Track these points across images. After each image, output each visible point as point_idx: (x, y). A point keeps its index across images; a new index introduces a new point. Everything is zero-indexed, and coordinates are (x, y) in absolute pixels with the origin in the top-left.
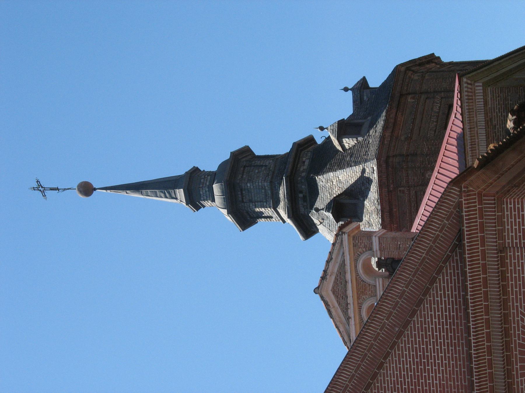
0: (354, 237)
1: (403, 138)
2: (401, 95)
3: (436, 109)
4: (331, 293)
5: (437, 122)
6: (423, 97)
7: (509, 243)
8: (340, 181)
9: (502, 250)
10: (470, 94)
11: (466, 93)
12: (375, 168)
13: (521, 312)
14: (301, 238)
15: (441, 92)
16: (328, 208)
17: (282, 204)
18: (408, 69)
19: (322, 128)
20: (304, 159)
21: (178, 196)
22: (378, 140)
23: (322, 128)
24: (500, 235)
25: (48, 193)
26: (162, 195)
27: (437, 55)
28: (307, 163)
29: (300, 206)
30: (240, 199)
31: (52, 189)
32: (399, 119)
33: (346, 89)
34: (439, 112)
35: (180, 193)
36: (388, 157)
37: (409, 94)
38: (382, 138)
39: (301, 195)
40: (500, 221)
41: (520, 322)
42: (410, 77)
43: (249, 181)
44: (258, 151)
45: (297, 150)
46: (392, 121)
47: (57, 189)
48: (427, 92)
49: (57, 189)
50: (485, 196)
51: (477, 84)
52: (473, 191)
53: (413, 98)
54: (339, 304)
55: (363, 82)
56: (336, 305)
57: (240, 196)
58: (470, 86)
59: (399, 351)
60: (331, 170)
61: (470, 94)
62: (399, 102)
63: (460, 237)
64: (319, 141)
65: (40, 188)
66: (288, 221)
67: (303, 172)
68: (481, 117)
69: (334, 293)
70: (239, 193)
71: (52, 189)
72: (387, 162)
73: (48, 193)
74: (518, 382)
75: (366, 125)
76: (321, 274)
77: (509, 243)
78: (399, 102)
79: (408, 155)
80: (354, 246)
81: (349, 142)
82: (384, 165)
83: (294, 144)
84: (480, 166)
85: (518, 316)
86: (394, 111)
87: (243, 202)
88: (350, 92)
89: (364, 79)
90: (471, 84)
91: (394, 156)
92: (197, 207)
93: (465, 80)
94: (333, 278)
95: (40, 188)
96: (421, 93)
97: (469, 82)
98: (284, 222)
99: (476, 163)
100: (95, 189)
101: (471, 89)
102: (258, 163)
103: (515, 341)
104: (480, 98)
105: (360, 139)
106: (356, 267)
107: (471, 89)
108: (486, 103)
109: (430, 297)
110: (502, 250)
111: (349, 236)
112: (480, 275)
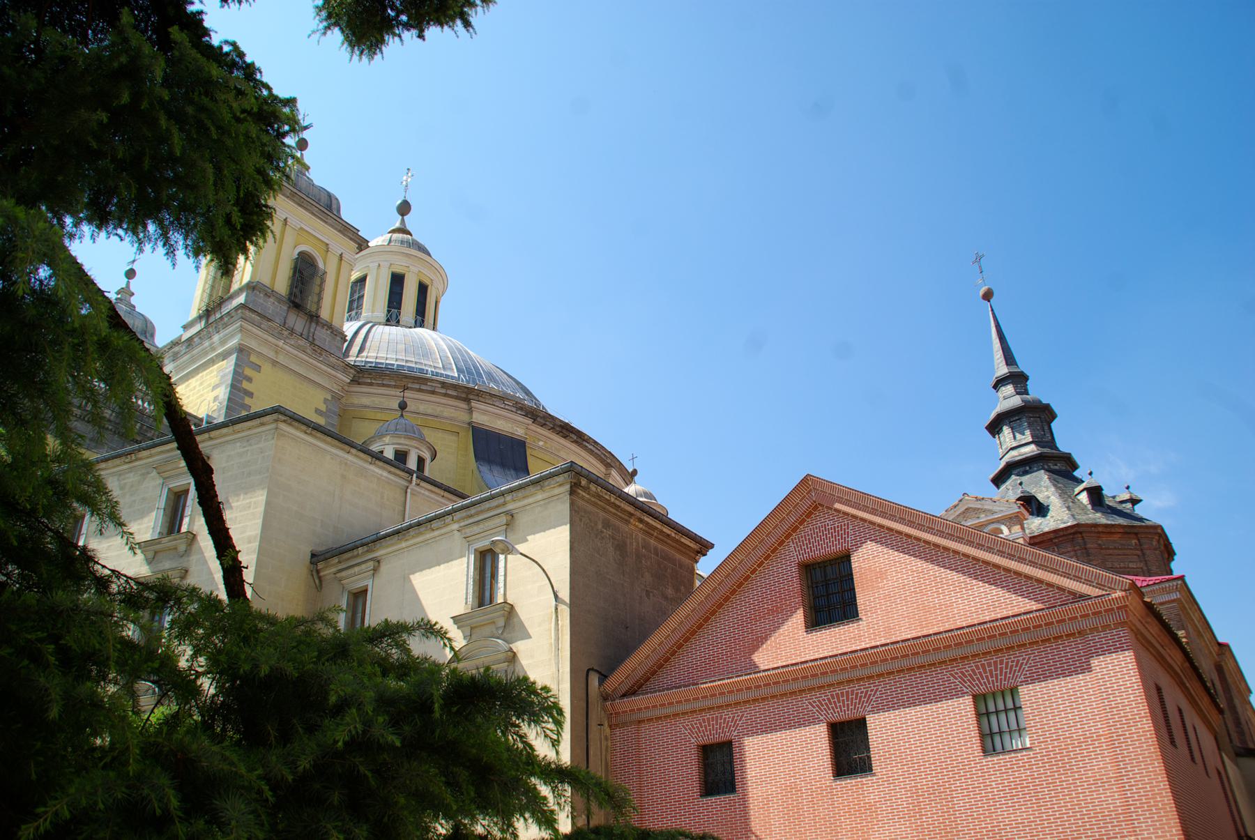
0: (1017, 516)
1: (1100, 542)
2: (1136, 534)
3: (1131, 565)
4: (966, 507)
5: (1121, 568)
6: (1139, 552)
7: (1088, 637)
8: (1049, 497)
9: (1081, 633)
10: (1168, 589)
11: (1167, 586)
12: (1069, 524)
13: (1029, 658)
14: (992, 476)
15: (1147, 566)
18: (1160, 535)
19: (1091, 474)
20: (1059, 465)
22: (1093, 522)
24: (1095, 629)
25: (976, 265)
27: (1175, 557)
29: (1018, 470)
30: (1012, 420)
32: (1115, 536)
34: (1128, 568)
36: (1081, 533)
37: (1138, 540)
38: (1096, 525)
39: (1028, 468)
41: (1021, 658)
42: (1153, 538)
44: (1054, 425)
45: (1066, 457)
46: (1113, 531)
48: (1144, 554)
50: (1126, 611)
51: (1178, 593)
52: (1128, 599)
53: (1136, 545)
54: (958, 516)
56: (957, 513)
57: (1014, 419)
58: (1175, 587)
59: (972, 565)
61: (1168, 589)
62: (1130, 533)
64: (1076, 473)
65: (979, 259)
66: (1002, 464)
67: (1048, 466)
69: (966, 509)
70: (1017, 418)
73: (976, 265)
74: (970, 664)
77: (1088, 637)
78: (1130, 533)
79: (1086, 549)
80: (1010, 518)
81: (1084, 497)
82: (1072, 531)
83: (1070, 454)
84: (1146, 603)
85: (1026, 655)
86: (1121, 530)
90: (1177, 588)
91: (1083, 537)
93: (1180, 582)
94: (979, 506)
95: (979, 259)
96: (1142, 550)
97: (1179, 586)
98: (1001, 459)
99: (1147, 599)
100: (989, 301)
101: (1173, 589)
102: (1046, 428)
103: (1005, 656)
105: (1089, 507)
106: (993, 523)
107: (1173, 589)
109: (1024, 582)
110: (1081, 633)
111: (1018, 512)
112: (1055, 618)
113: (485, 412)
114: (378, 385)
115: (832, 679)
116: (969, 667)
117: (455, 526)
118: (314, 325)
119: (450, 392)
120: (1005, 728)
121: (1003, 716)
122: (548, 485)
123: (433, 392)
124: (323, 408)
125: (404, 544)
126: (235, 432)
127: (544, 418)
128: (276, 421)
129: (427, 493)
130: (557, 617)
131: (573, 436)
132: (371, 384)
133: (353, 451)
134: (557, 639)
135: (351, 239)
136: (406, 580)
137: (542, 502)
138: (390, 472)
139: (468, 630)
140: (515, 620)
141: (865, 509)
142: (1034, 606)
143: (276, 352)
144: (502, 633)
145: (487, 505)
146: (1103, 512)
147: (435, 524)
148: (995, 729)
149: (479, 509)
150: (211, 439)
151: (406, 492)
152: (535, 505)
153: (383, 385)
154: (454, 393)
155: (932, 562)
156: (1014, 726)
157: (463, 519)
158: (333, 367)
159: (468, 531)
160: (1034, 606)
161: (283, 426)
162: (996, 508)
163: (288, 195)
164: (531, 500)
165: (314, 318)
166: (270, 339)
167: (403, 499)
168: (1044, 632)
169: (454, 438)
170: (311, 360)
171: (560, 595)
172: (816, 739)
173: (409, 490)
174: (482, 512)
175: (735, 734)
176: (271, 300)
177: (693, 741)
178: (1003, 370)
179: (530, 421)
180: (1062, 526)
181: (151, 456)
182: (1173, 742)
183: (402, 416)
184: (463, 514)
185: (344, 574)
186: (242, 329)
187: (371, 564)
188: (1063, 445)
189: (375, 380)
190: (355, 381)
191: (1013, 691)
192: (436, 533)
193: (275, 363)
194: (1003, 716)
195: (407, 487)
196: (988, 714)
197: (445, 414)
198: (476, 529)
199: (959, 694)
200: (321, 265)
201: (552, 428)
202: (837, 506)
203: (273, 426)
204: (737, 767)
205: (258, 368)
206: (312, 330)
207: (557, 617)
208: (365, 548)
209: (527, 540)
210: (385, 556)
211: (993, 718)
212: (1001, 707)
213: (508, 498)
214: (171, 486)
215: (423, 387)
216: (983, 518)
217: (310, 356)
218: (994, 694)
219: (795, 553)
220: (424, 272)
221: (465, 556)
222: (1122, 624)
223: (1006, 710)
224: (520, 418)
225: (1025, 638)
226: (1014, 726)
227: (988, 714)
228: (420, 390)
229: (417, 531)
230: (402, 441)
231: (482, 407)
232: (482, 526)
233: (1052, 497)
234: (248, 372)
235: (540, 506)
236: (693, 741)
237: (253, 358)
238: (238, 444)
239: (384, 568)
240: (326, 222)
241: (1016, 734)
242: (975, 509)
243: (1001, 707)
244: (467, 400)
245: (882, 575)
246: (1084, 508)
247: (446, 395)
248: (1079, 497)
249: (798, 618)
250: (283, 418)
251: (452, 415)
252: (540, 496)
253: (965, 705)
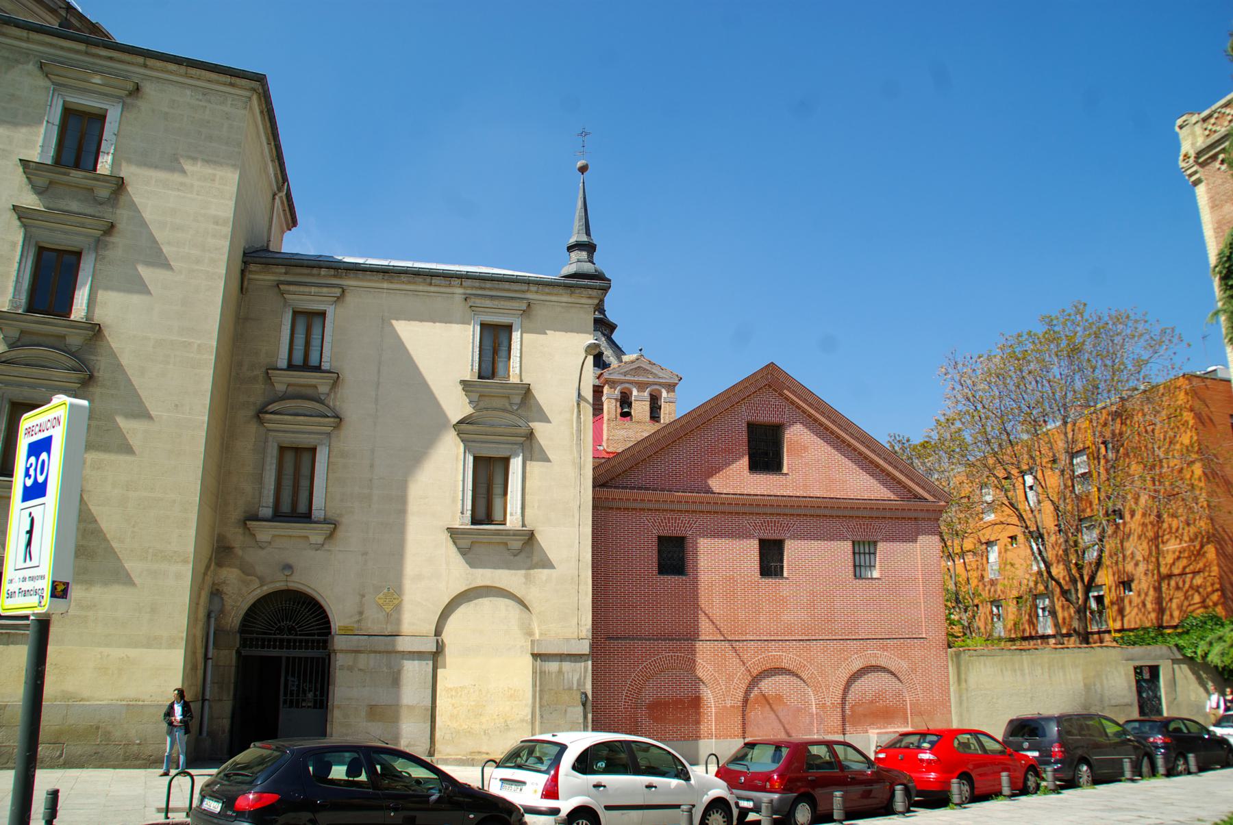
35: (584, 238)
40: (929, 519)
54: (632, 369)
73: (581, 139)
76: (653, 361)
94: (649, 368)
115: (769, 510)
116: (853, 523)
117: (460, 291)
120: (863, 564)
121: (862, 556)
122: (580, 293)
125: (385, 285)
126: (186, 75)
128: (254, 90)
130: (579, 411)
134: (579, 431)
136: (384, 323)
137: (564, 304)
139: (475, 397)
140: (532, 401)
141: (805, 401)
142: (893, 497)
144: (517, 410)
145: (507, 286)
147: (435, 280)
149: (497, 286)
150: (145, 66)
152: (556, 304)
155: (838, 450)
156: (868, 564)
157: (472, 288)
159: (478, 302)
160: (893, 497)
162: (661, 375)
164: (554, 298)
168: (899, 514)
171: (583, 393)
172: (750, 549)
174: (497, 289)
175: (690, 533)
177: (654, 532)
178: (577, 237)
181: (28, 40)
184: (477, 283)
185: (292, 288)
187: (338, 292)
191: (875, 543)
192: (432, 289)
194: (862, 556)
198: (488, 303)
199: (844, 539)
202: (785, 391)
203: (248, 94)
204: (690, 556)
207: (579, 411)
208: (332, 272)
209: (546, 334)
210: (351, 288)
213: (533, 288)
214: (68, 99)
216: (651, 379)
218: (864, 542)
219: (746, 414)
221: (470, 324)
225: (888, 514)
226: (868, 564)
229: (411, 279)
232: (496, 303)
235: (562, 307)
236: (654, 532)
238: (188, 92)
239: (350, 299)
241: (868, 569)
242: (645, 369)
245: (805, 448)
249: (745, 461)
252: (565, 299)
253: (848, 545)
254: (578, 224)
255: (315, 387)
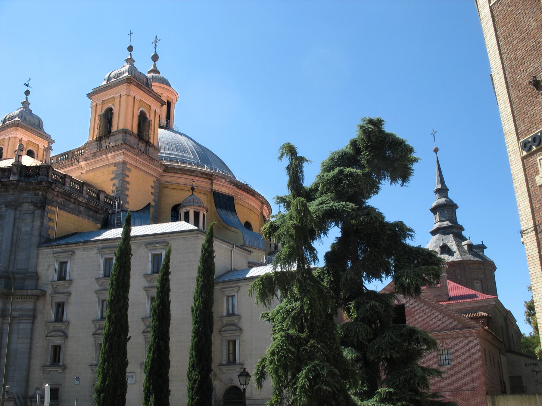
8: (452, 246)
9: (467, 337)
12: (459, 259)
16: (443, 244)
17: (441, 223)
19: (469, 238)
21: (438, 185)
23: (469, 238)
26: (438, 179)
28: (456, 231)
31: (434, 137)
33: (482, 242)
35: (440, 186)
36: (463, 263)
38: (469, 261)
39: (445, 230)
43: (447, 211)
47: (434, 139)
48: (485, 272)
49: (434, 139)
55: (486, 248)
60: (456, 242)
63: (470, 328)
68: (485, 304)
71: (434, 137)
72: (462, 263)
75: (472, 253)
81: (466, 247)
83: (462, 226)
87: (440, 210)
88: (482, 243)
89: (486, 248)
92: (435, 192)
95: (434, 133)
98: (434, 224)
102: (454, 213)
104: (490, 303)
105: (467, 252)
108: (489, 305)
110: (467, 337)
113: (218, 185)
114: (174, 173)
118: (148, 147)
119: (204, 176)
123: (197, 176)
124: (153, 185)
126: (179, 235)
127: (241, 186)
128: (197, 234)
129: (237, 251)
131: (251, 192)
132: (171, 172)
133: (218, 240)
135: (159, 102)
138: (228, 246)
143: (136, 162)
146: (472, 255)
148: (442, 359)
150: (169, 236)
151: (232, 252)
153: (176, 173)
154: (206, 177)
158: (157, 166)
161: (200, 235)
163: (135, 84)
165: (148, 143)
166: (134, 156)
167: (231, 254)
169: (205, 196)
170: (149, 164)
173: (232, 251)
176: (132, 137)
179: (235, 188)
180: (457, 260)
182: (486, 364)
183: (193, 193)
185: (225, 290)
186: (124, 154)
187: (237, 288)
188: (460, 222)
189: (173, 171)
190: (165, 171)
193: (136, 167)
194: (444, 356)
195: (232, 250)
196: (440, 355)
197: (201, 185)
200: (148, 117)
201: (243, 190)
203: (197, 235)
205: (130, 170)
206: (148, 149)
208: (234, 282)
211: (442, 356)
212: (444, 353)
214: (152, 253)
215: (193, 174)
217: (148, 162)
220: (170, 96)
222: (478, 336)
223: (445, 354)
224: (231, 187)
227: (440, 355)
228: (192, 175)
230: (197, 208)
231: (217, 182)
233: (454, 246)
234: (127, 173)
237: (128, 166)
238: (181, 240)
239: (241, 289)
240: (149, 95)
243: (444, 353)
244: (211, 180)
246: (465, 252)
247: (203, 177)
248: (464, 247)
250: (200, 232)
251: (204, 186)
254: (436, 179)
255: (234, 321)
